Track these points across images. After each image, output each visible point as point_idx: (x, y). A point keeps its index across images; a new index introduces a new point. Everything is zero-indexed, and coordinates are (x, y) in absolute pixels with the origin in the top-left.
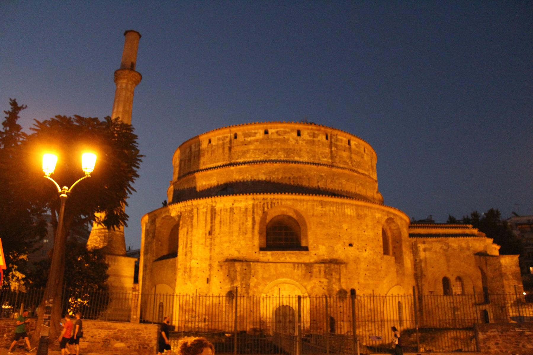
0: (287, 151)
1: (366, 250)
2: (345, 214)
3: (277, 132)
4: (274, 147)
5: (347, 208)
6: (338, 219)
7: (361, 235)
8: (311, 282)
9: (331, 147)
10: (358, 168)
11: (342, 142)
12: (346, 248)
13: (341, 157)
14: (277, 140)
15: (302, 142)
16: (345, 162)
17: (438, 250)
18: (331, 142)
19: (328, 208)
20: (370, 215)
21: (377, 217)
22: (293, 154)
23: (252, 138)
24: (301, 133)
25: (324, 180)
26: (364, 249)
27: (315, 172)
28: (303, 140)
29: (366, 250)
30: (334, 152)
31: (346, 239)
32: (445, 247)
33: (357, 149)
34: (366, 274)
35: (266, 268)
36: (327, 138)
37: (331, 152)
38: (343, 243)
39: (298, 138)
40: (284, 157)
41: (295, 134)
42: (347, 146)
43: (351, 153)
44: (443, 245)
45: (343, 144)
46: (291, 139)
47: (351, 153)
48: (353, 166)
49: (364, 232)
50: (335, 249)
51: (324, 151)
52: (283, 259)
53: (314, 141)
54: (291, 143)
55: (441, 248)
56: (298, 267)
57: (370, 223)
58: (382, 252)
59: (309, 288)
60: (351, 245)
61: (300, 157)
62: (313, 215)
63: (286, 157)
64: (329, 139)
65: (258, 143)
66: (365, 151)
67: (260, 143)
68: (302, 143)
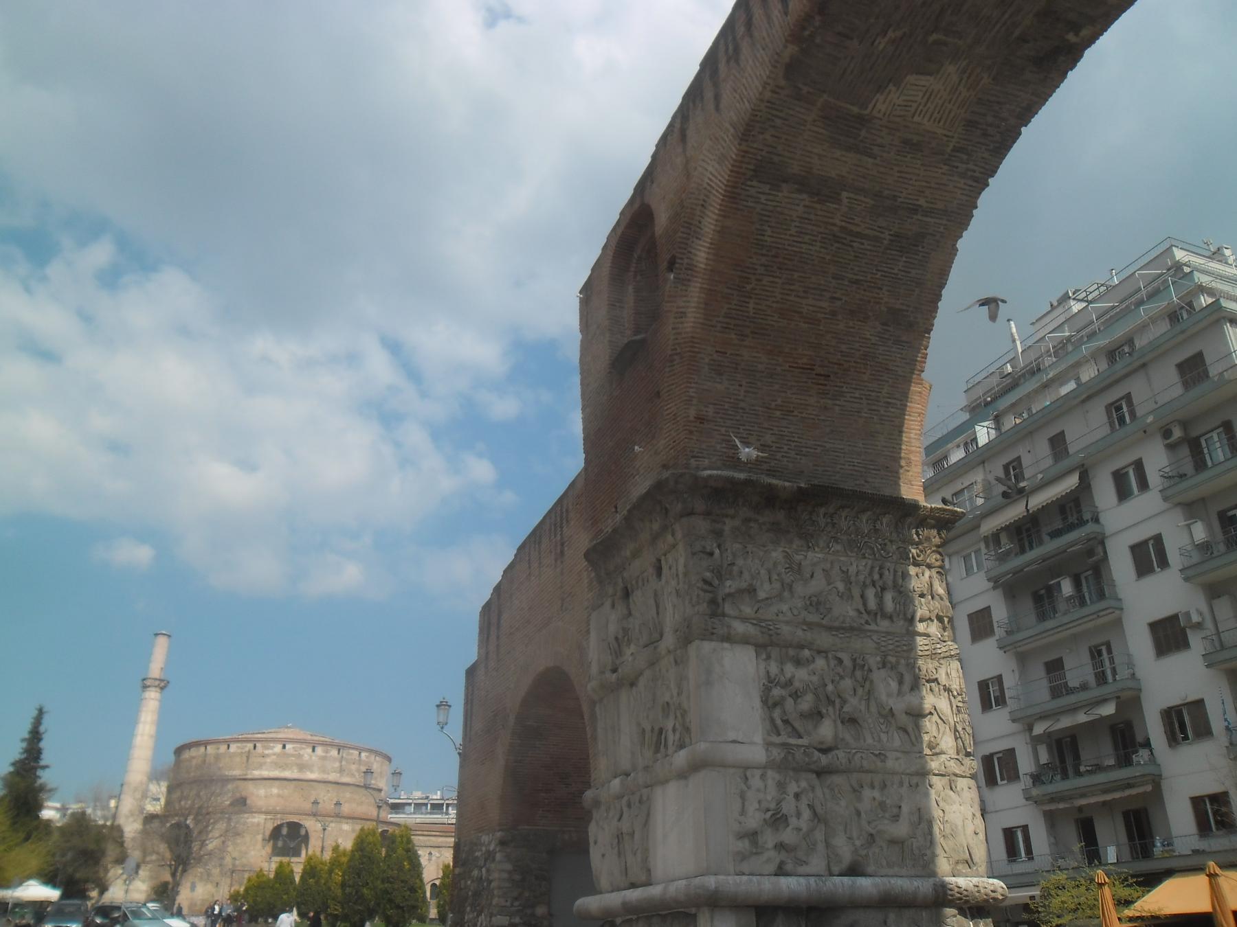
0: (302, 767)
9: (341, 762)
14: (293, 755)
16: (352, 774)
18: (342, 757)
23: (270, 751)
24: (316, 749)
28: (317, 756)
33: (367, 760)
36: (339, 753)
37: (341, 766)
39: (312, 754)
41: (310, 750)
42: (357, 758)
43: (360, 764)
46: (306, 756)
47: (360, 764)
61: (312, 772)
65: (275, 757)
66: (375, 759)
67: (277, 757)
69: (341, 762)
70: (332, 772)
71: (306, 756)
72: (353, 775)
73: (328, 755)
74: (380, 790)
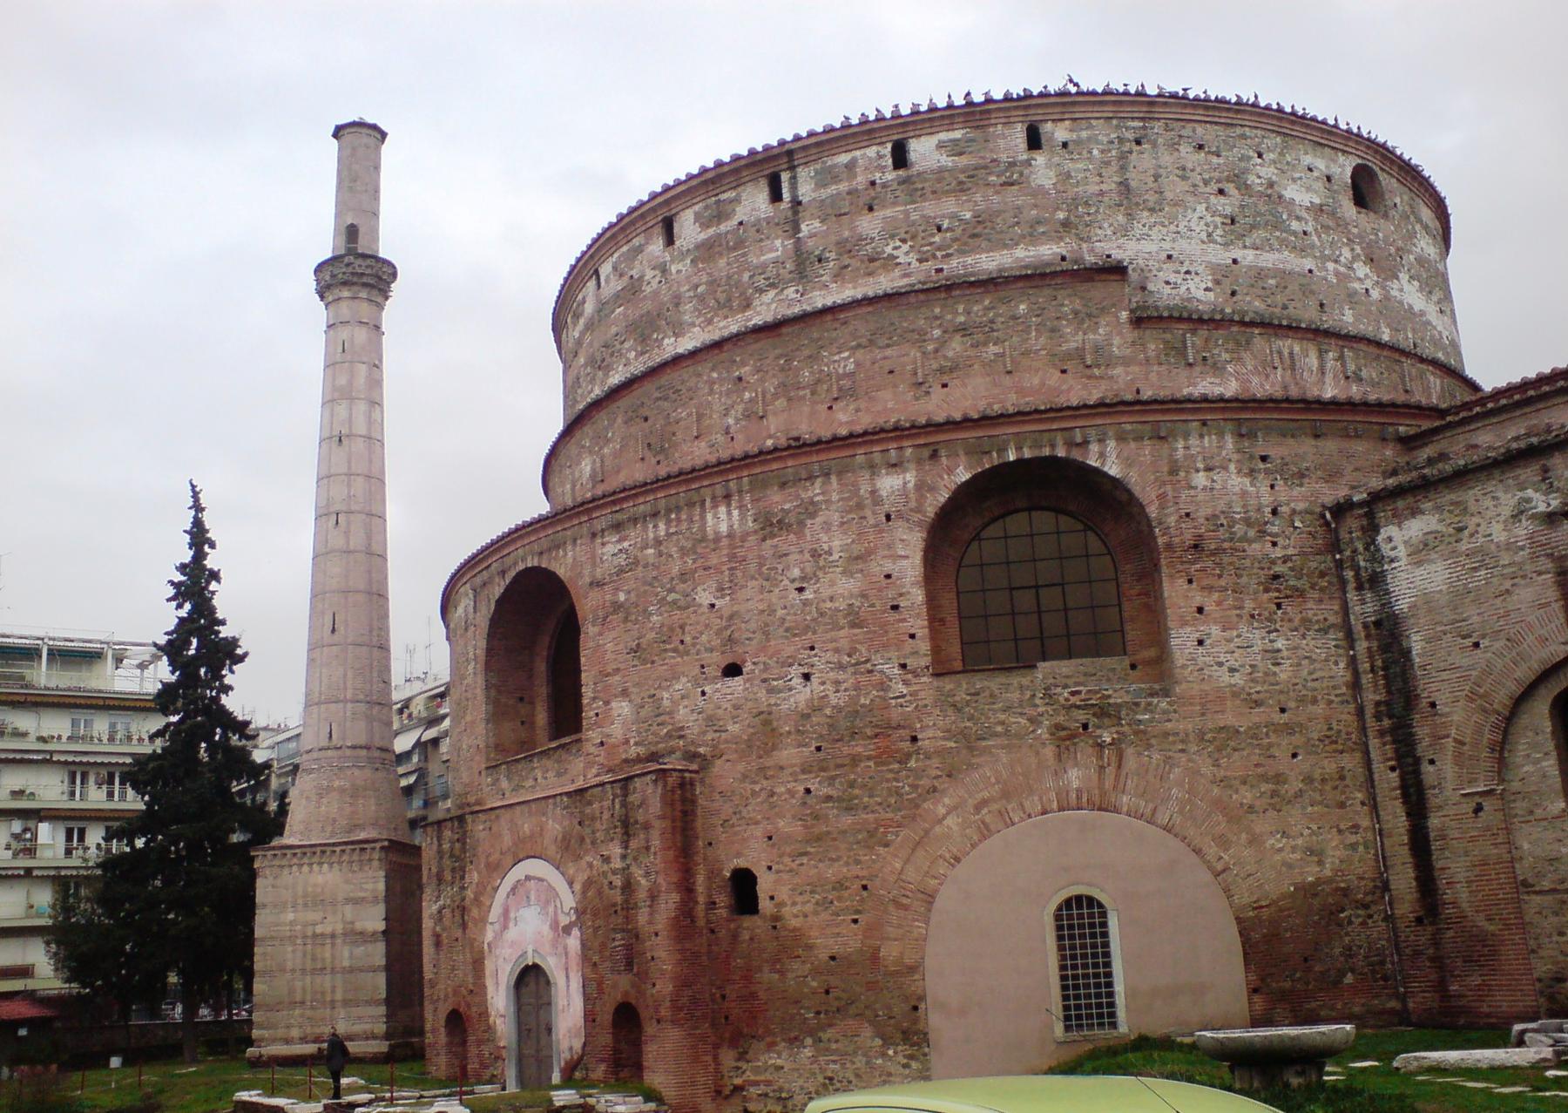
0: (644, 330)
1: (807, 677)
2: (704, 539)
3: (615, 268)
4: (614, 330)
5: (715, 507)
6: (675, 571)
7: (780, 613)
8: (583, 863)
10: (962, 252)
11: (855, 176)
12: (707, 689)
13: (847, 248)
14: (618, 298)
15: (680, 267)
17: (1499, 533)
18: (796, 203)
19: (634, 534)
20: (835, 497)
21: (884, 494)
22: (657, 329)
25: (747, 395)
26: (795, 671)
27: (715, 375)
28: (682, 256)
29: (807, 677)
30: (811, 243)
31: (712, 650)
32: (1542, 503)
33: (963, 161)
34: (808, 791)
35: (495, 829)
36: (776, 196)
38: (697, 670)
40: (636, 357)
41: (656, 246)
42: (891, 175)
44: (1530, 492)
45: (861, 180)
46: (649, 274)
48: (920, 261)
49: (801, 590)
50: (666, 703)
51: (763, 258)
52: (530, 783)
53: (720, 235)
54: (649, 289)
55: (1516, 516)
56: (555, 804)
57: (836, 543)
58: (925, 661)
59: (578, 887)
60: (733, 670)
61: (678, 331)
62: (591, 584)
63: (643, 353)
64: (786, 195)
66: (1034, 141)
68: (679, 272)
69: (797, 229)
70: (761, 291)
71: (649, 274)
72: (877, 262)
73: (723, 228)
74: (1116, 271)
